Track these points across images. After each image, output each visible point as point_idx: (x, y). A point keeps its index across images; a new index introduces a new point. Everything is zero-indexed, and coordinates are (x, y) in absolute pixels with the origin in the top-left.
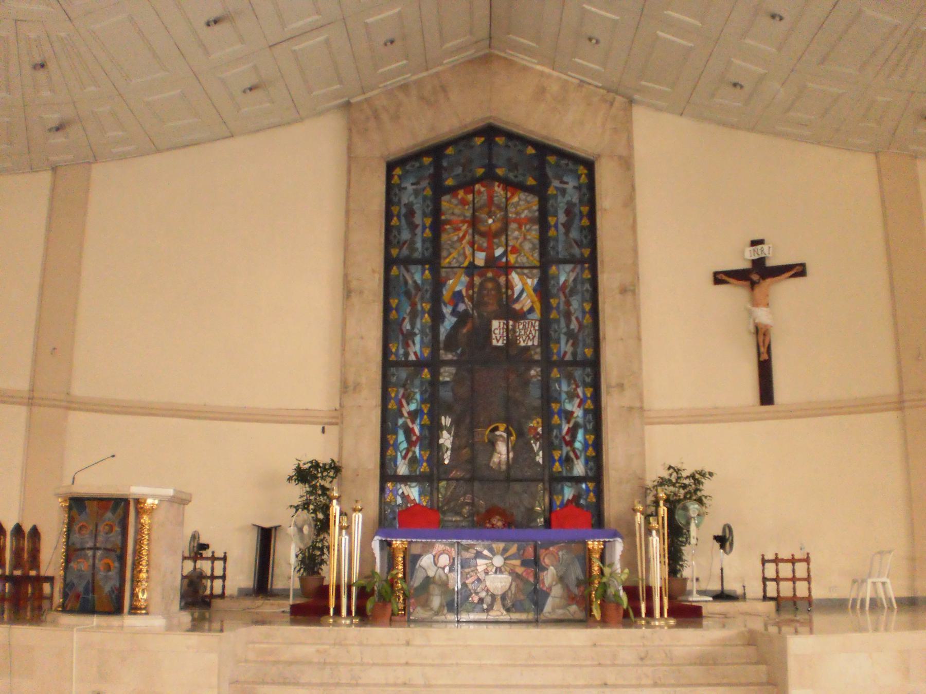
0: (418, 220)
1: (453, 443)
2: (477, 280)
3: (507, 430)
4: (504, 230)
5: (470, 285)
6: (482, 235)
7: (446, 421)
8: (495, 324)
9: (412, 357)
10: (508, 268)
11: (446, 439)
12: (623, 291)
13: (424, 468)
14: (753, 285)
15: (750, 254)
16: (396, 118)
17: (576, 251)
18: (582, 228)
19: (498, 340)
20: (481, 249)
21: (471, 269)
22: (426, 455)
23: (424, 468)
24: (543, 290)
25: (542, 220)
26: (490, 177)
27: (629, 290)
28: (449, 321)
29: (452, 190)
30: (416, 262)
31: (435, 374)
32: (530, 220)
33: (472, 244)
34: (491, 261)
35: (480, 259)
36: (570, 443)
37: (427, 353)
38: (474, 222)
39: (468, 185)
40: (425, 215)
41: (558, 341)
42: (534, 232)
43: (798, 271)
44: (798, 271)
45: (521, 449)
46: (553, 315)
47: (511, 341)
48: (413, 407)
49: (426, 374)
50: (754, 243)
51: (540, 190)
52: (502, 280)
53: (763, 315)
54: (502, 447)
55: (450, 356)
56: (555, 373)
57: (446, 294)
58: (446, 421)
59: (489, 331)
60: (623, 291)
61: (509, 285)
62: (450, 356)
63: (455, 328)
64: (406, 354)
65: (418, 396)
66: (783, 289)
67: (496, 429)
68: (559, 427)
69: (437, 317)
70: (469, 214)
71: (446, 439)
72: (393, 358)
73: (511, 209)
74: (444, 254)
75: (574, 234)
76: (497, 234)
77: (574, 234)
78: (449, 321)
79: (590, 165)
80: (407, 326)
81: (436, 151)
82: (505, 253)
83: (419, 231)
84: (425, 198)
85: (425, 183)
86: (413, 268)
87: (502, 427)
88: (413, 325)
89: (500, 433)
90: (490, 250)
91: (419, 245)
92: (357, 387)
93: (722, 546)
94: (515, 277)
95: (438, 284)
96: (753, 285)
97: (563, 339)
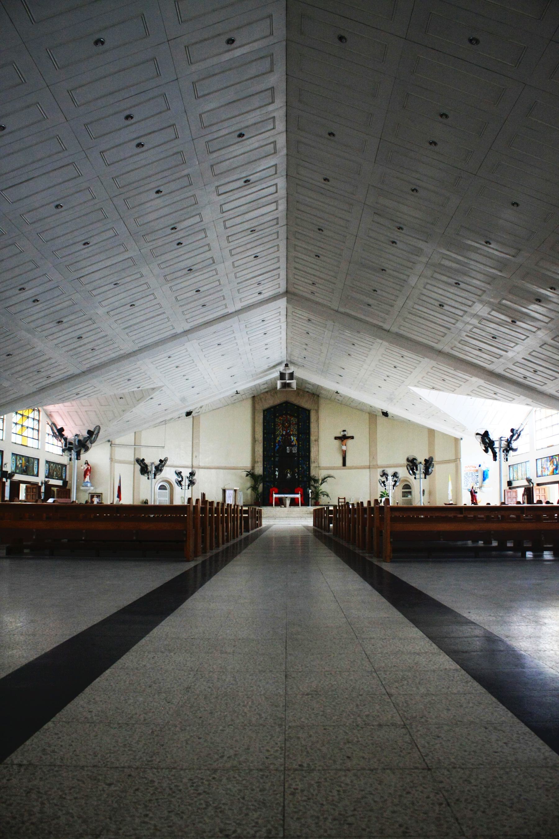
4: (289, 426)
5: (282, 439)
6: (285, 427)
7: (277, 469)
10: (290, 435)
11: (277, 473)
12: (315, 441)
14: (342, 441)
15: (342, 433)
16: (265, 400)
21: (282, 435)
24: (298, 440)
25: (298, 424)
26: (286, 414)
27: (317, 440)
28: (277, 448)
29: (278, 417)
32: (295, 424)
33: (282, 429)
38: (283, 424)
39: (281, 416)
43: (352, 438)
44: (352, 438)
45: (293, 475)
50: (344, 431)
51: (297, 417)
53: (344, 448)
54: (289, 475)
57: (277, 441)
59: (286, 449)
60: (315, 441)
61: (291, 439)
63: (279, 448)
66: (349, 442)
69: (275, 446)
71: (277, 473)
78: (277, 448)
79: (309, 411)
81: (274, 407)
90: (286, 432)
92: (258, 462)
94: (292, 437)
96: (342, 441)
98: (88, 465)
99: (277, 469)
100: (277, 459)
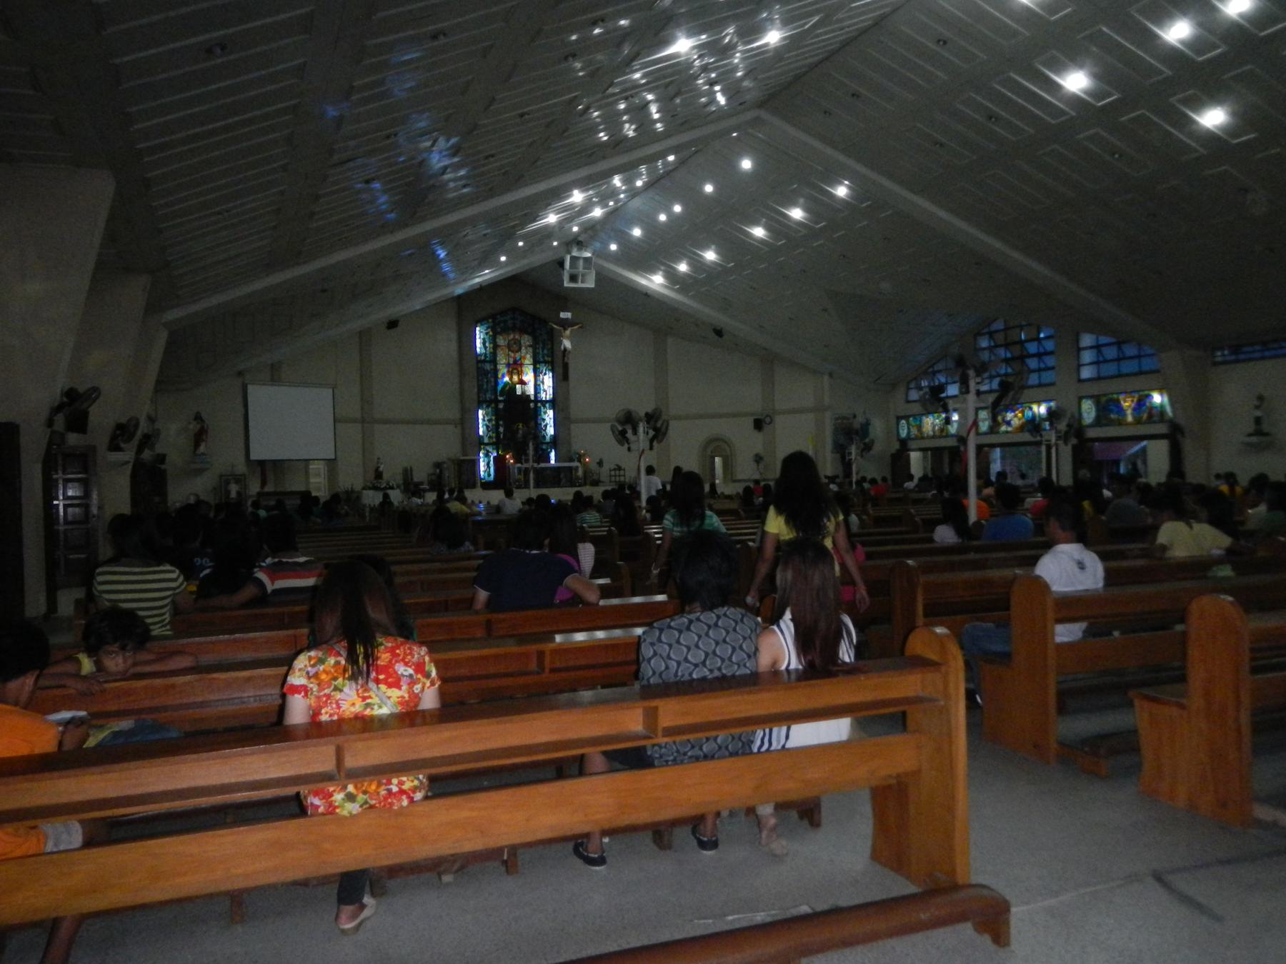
0: (487, 345)
1: (504, 431)
2: (510, 369)
3: (523, 426)
4: (520, 350)
6: (513, 352)
8: (518, 386)
9: (488, 399)
11: (501, 429)
13: (494, 440)
17: (546, 358)
18: (548, 350)
19: (519, 392)
20: (511, 357)
22: (494, 435)
23: (494, 440)
28: (500, 387)
29: (500, 333)
30: (487, 362)
31: (497, 406)
32: (530, 346)
34: (515, 362)
35: (511, 362)
36: (545, 430)
37: (493, 397)
40: (490, 343)
41: (540, 393)
42: (530, 350)
46: (538, 383)
47: (523, 393)
48: (489, 418)
49: (493, 405)
52: (520, 369)
55: (501, 398)
56: (539, 405)
57: (500, 376)
58: (501, 423)
62: (501, 398)
64: (486, 397)
65: (490, 414)
67: (519, 425)
68: (541, 424)
69: (496, 384)
70: (506, 343)
71: (501, 429)
72: (481, 399)
73: (522, 342)
74: (498, 359)
75: (545, 352)
76: (517, 352)
77: (545, 352)
80: (485, 387)
82: (520, 359)
83: (488, 349)
84: (490, 336)
85: (489, 330)
86: (486, 364)
87: (521, 425)
88: (487, 385)
89: (521, 426)
91: (488, 355)
93: (600, 466)
95: (496, 371)
97: (542, 392)
98: (202, 420)
99: (501, 423)
100: (501, 406)
